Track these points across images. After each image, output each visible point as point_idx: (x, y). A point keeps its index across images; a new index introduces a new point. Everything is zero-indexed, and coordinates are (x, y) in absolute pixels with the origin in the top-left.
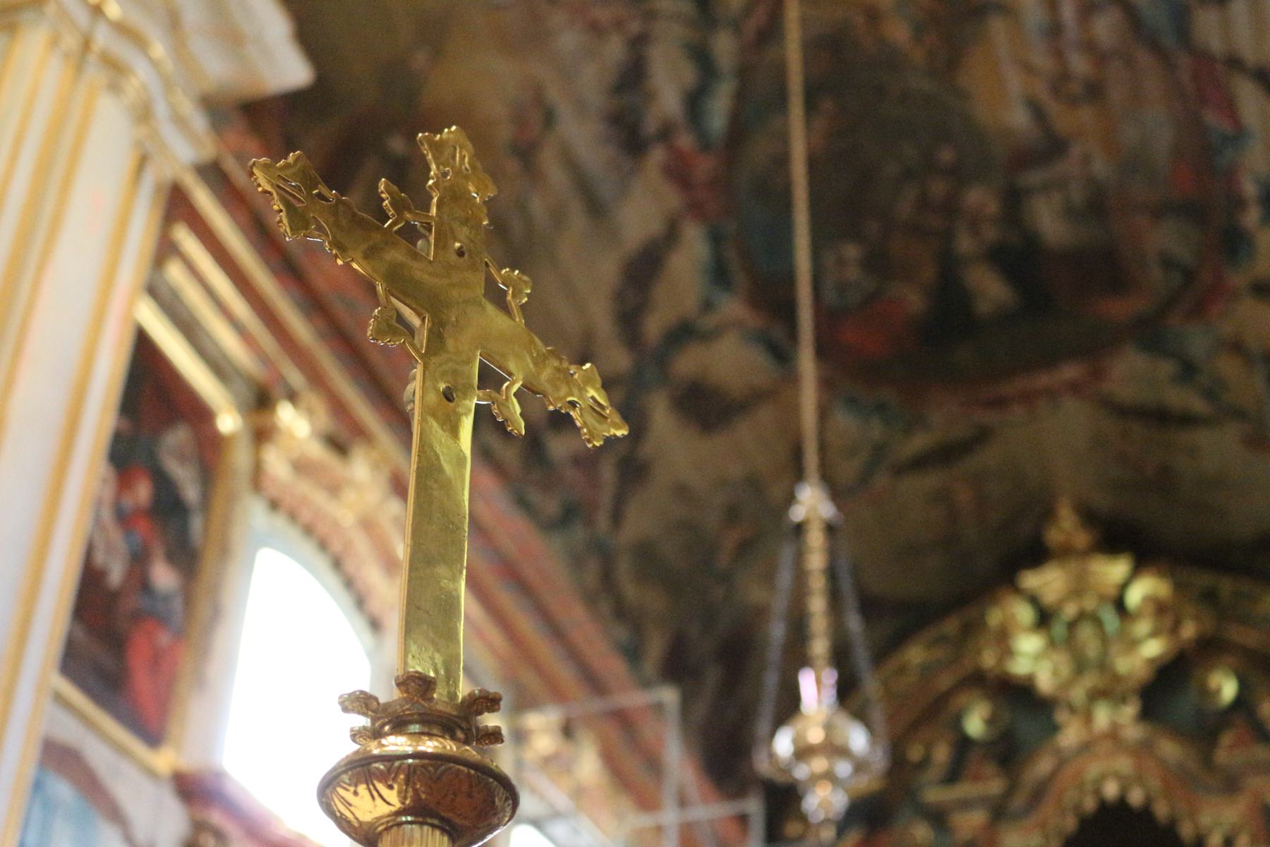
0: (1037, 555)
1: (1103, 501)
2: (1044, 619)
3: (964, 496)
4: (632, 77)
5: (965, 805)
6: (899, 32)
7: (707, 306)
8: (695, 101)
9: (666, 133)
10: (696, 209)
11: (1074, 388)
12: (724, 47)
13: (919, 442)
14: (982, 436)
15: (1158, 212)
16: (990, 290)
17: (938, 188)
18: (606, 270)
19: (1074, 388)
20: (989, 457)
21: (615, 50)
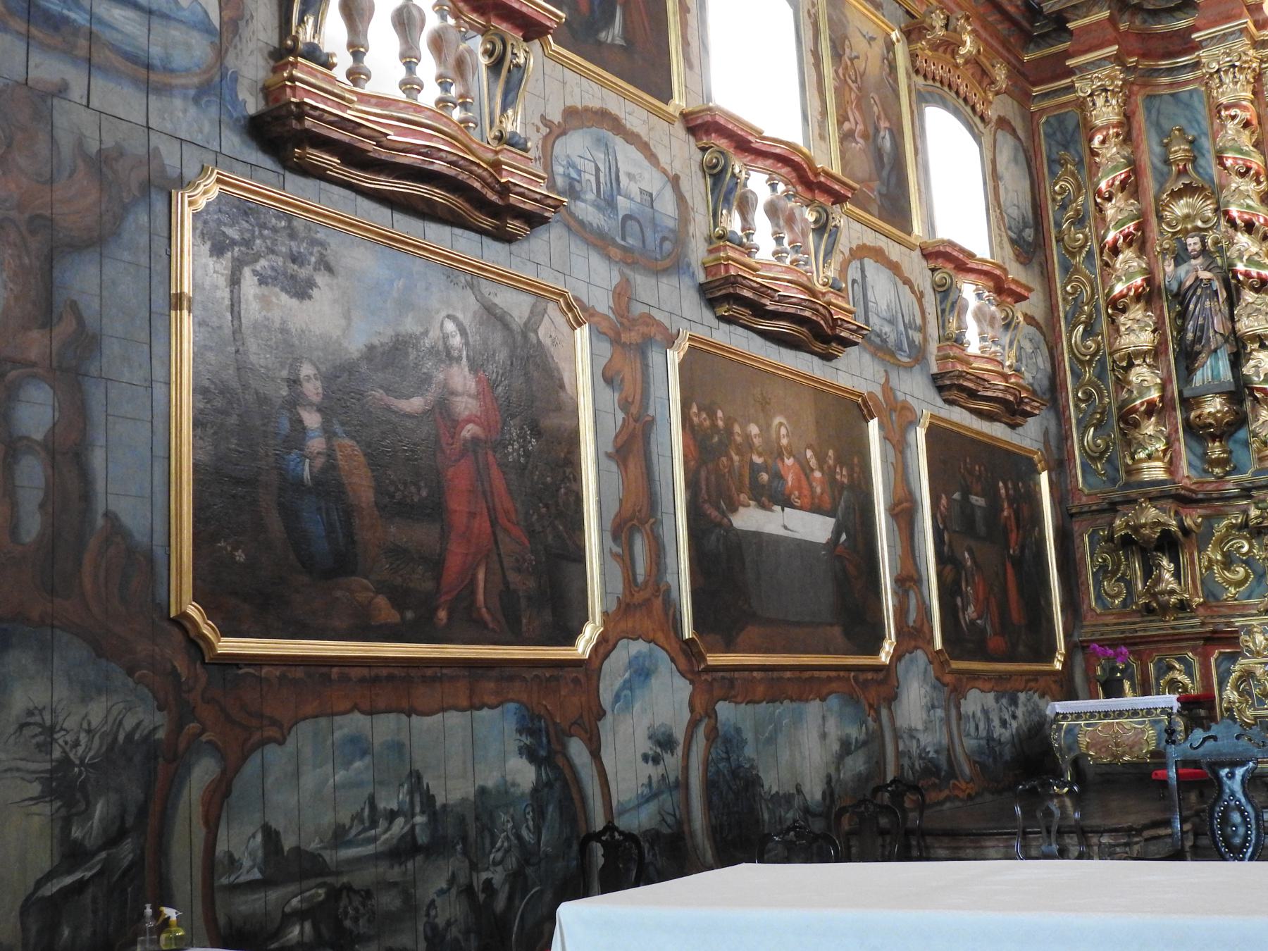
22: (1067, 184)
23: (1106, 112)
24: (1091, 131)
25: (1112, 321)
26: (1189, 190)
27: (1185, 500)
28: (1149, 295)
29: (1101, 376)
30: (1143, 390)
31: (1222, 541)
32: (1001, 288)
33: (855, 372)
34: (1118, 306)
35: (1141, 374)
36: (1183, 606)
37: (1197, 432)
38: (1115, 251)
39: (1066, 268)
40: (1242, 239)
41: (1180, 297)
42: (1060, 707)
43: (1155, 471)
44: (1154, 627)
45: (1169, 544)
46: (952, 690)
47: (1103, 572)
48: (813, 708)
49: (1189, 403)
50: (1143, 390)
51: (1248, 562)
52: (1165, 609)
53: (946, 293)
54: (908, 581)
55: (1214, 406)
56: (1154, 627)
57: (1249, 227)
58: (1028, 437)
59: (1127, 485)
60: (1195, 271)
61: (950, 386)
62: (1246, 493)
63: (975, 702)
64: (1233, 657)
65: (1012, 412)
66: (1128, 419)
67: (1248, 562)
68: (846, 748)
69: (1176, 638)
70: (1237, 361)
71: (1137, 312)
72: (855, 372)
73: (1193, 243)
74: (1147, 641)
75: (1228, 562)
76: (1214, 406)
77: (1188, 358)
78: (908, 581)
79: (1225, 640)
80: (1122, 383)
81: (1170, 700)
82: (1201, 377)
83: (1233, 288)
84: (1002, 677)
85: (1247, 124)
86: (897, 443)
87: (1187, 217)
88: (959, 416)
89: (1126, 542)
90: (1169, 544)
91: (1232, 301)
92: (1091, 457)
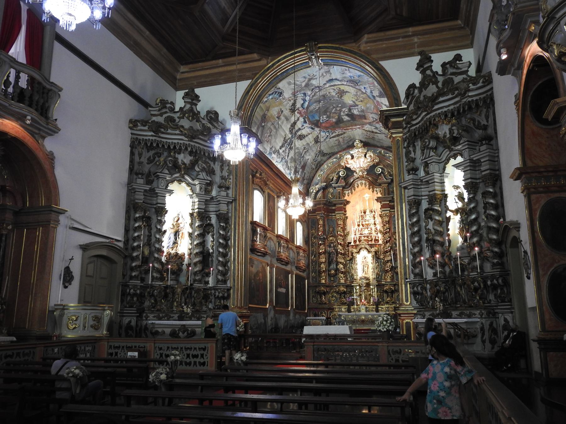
0: (352, 146)
1: (363, 140)
2: (353, 157)
3: (341, 140)
4: (294, 104)
5: (339, 187)
6: (334, 94)
7: (303, 126)
8: (302, 105)
9: (298, 109)
10: (302, 116)
11: (359, 128)
12: (307, 98)
13: (334, 134)
14: (344, 133)
15: (372, 113)
16: (346, 118)
17: (338, 109)
18: (289, 126)
19: (359, 128)
20: (345, 135)
21: (292, 102)
22: (314, 231)
23: (321, 222)
24: (319, 224)
25: (319, 256)
26: (332, 236)
27: (327, 286)
28: (324, 253)
29: (316, 264)
30: (323, 268)
31: (332, 293)
32: (304, 251)
33: (288, 268)
34: (320, 254)
35: (322, 265)
36: (325, 303)
37: (330, 275)
38: (321, 245)
39: (312, 245)
40: (339, 246)
41: (329, 254)
42: (308, 318)
43: (323, 281)
44: (321, 306)
45: (325, 293)
46: (295, 314)
47: (313, 297)
48: (283, 316)
49: (329, 271)
50: (323, 268)
51: (335, 297)
52: (323, 303)
53: (298, 253)
54: (292, 298)
55: (333, 272)
56: (321, 306)
57: (341, 244)
58: (304, 275)
59: (319, 283)
60: (332, 250)
61: (298, 268)
62: (336, 286)
63: (297, 316)
64: (332, 312)
65: (304, 271)
66: (320, 272)
67: (335, 297)
68: (285, 321)
69: (324, 309)
70: (337, 265)
71: (323, 255)
72: (288, 268)
73: (332, 245)
74: (320, 308)
75: (332, 297)
76: (333, 272)
77: (330, 263)
78: (292, 298)
79: (332, 309)
80: (320, 266)
81: (325, 318)
82: (331, 267)
83: (337, 253)
84: (300, 313)
85: (342, 228)
86: (292, 277)
87: (331, 240)
88: (298, 272)
89: (318, 292)
90: (325, 293)
91: (337, 255)
92: (313, 277)
